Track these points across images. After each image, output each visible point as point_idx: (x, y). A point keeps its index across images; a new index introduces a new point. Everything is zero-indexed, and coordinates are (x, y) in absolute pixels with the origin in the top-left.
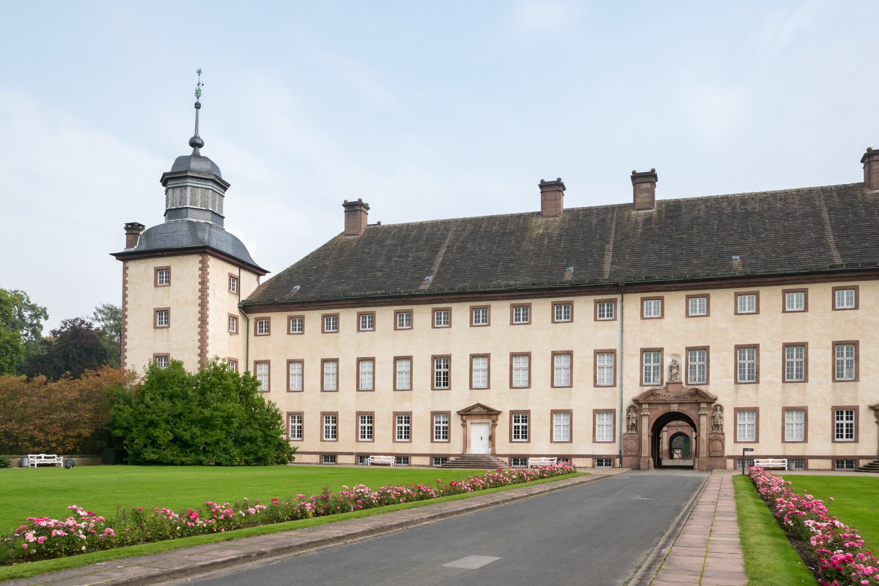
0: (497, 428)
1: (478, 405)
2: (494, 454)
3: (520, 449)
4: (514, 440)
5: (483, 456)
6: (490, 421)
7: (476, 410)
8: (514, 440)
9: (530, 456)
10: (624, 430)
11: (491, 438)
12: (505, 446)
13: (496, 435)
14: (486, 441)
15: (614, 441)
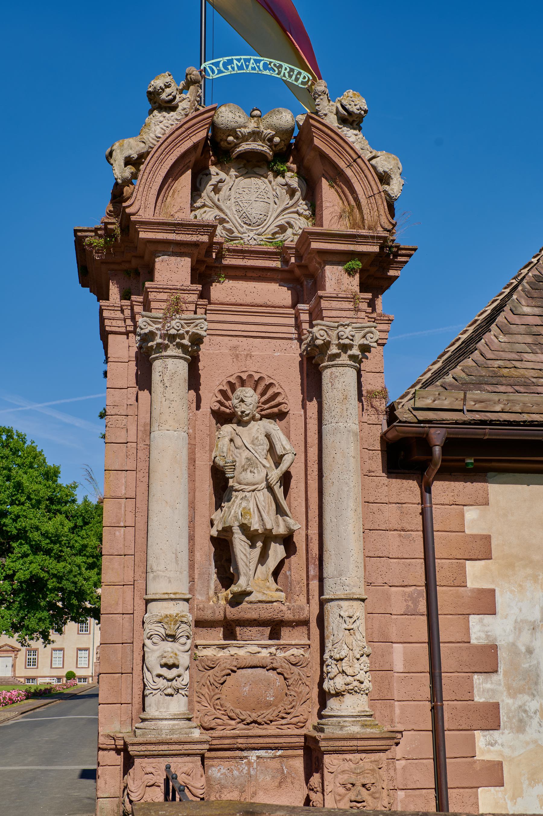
0: (17, 659)
1: (6, 645)
2: (15, 677)
3: (31, 673)
4: (27, 667)
5: (9, 678)
6: (13, 655)
7: (4, 648)
8: (27, 667)
9: (38, 677)
10: (95, 660)
11: (13, 666)
12: (22, 672)
13: (17, 663)
14: (10, 668)
15: (88, 667)
